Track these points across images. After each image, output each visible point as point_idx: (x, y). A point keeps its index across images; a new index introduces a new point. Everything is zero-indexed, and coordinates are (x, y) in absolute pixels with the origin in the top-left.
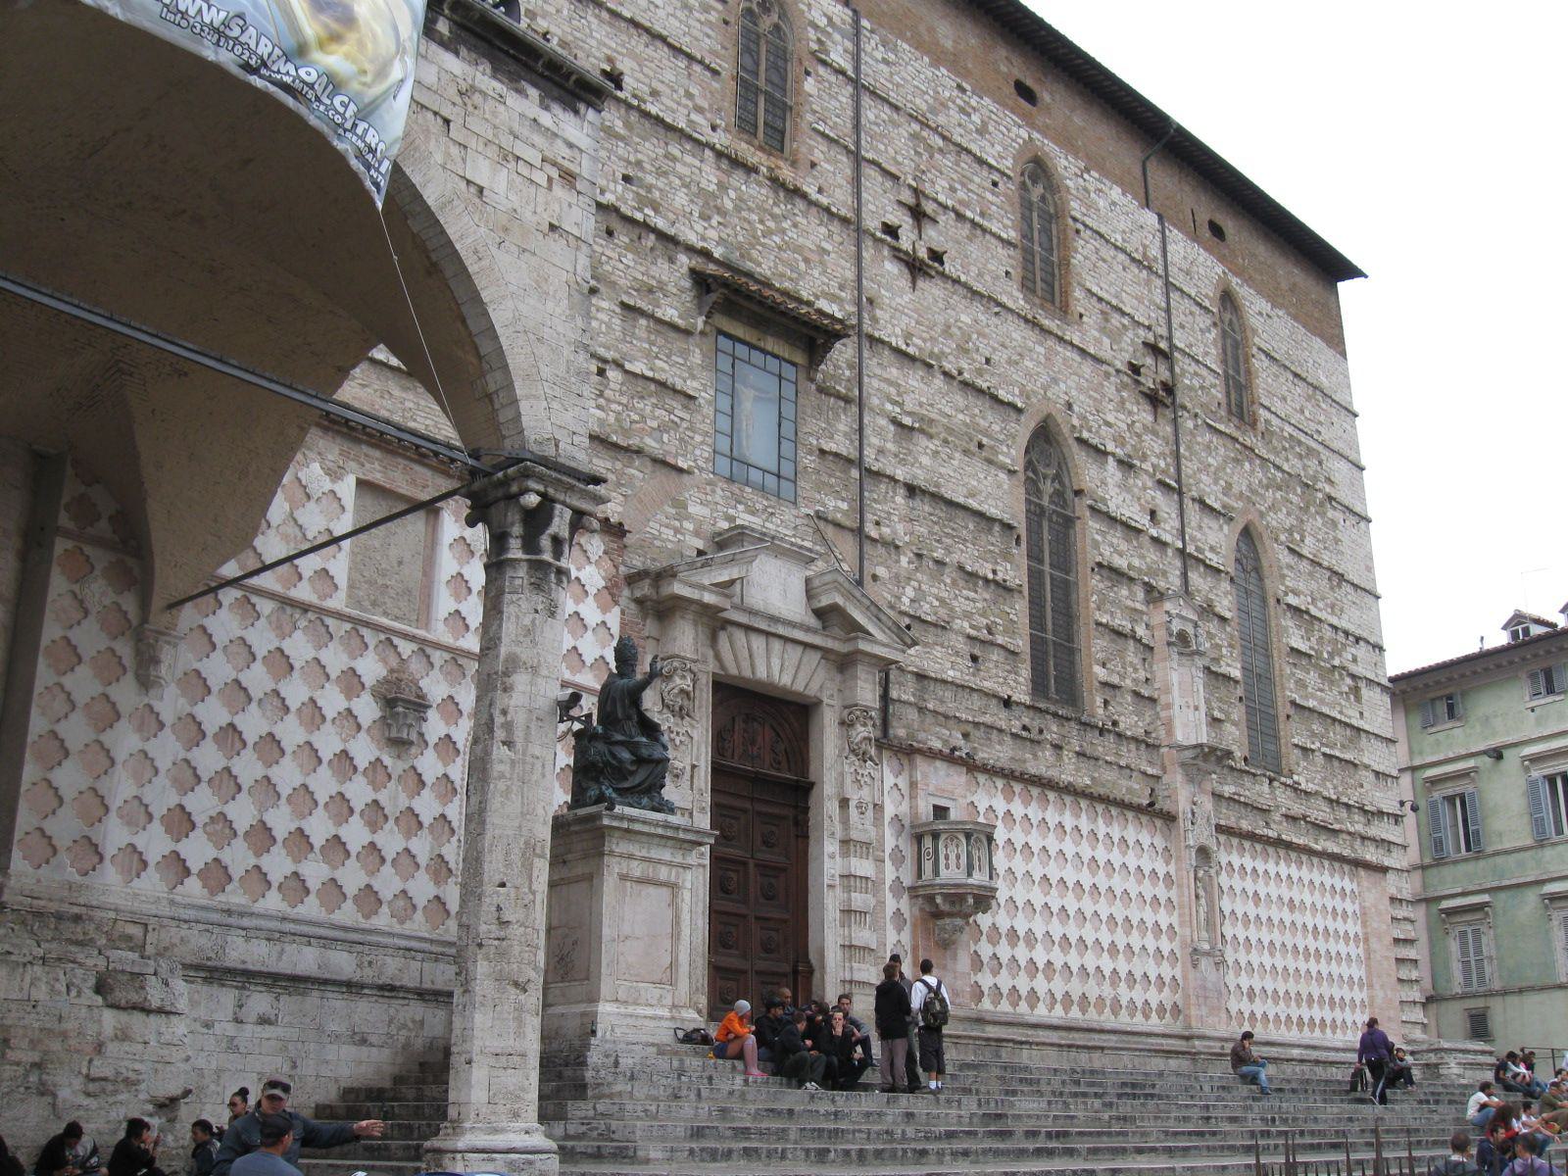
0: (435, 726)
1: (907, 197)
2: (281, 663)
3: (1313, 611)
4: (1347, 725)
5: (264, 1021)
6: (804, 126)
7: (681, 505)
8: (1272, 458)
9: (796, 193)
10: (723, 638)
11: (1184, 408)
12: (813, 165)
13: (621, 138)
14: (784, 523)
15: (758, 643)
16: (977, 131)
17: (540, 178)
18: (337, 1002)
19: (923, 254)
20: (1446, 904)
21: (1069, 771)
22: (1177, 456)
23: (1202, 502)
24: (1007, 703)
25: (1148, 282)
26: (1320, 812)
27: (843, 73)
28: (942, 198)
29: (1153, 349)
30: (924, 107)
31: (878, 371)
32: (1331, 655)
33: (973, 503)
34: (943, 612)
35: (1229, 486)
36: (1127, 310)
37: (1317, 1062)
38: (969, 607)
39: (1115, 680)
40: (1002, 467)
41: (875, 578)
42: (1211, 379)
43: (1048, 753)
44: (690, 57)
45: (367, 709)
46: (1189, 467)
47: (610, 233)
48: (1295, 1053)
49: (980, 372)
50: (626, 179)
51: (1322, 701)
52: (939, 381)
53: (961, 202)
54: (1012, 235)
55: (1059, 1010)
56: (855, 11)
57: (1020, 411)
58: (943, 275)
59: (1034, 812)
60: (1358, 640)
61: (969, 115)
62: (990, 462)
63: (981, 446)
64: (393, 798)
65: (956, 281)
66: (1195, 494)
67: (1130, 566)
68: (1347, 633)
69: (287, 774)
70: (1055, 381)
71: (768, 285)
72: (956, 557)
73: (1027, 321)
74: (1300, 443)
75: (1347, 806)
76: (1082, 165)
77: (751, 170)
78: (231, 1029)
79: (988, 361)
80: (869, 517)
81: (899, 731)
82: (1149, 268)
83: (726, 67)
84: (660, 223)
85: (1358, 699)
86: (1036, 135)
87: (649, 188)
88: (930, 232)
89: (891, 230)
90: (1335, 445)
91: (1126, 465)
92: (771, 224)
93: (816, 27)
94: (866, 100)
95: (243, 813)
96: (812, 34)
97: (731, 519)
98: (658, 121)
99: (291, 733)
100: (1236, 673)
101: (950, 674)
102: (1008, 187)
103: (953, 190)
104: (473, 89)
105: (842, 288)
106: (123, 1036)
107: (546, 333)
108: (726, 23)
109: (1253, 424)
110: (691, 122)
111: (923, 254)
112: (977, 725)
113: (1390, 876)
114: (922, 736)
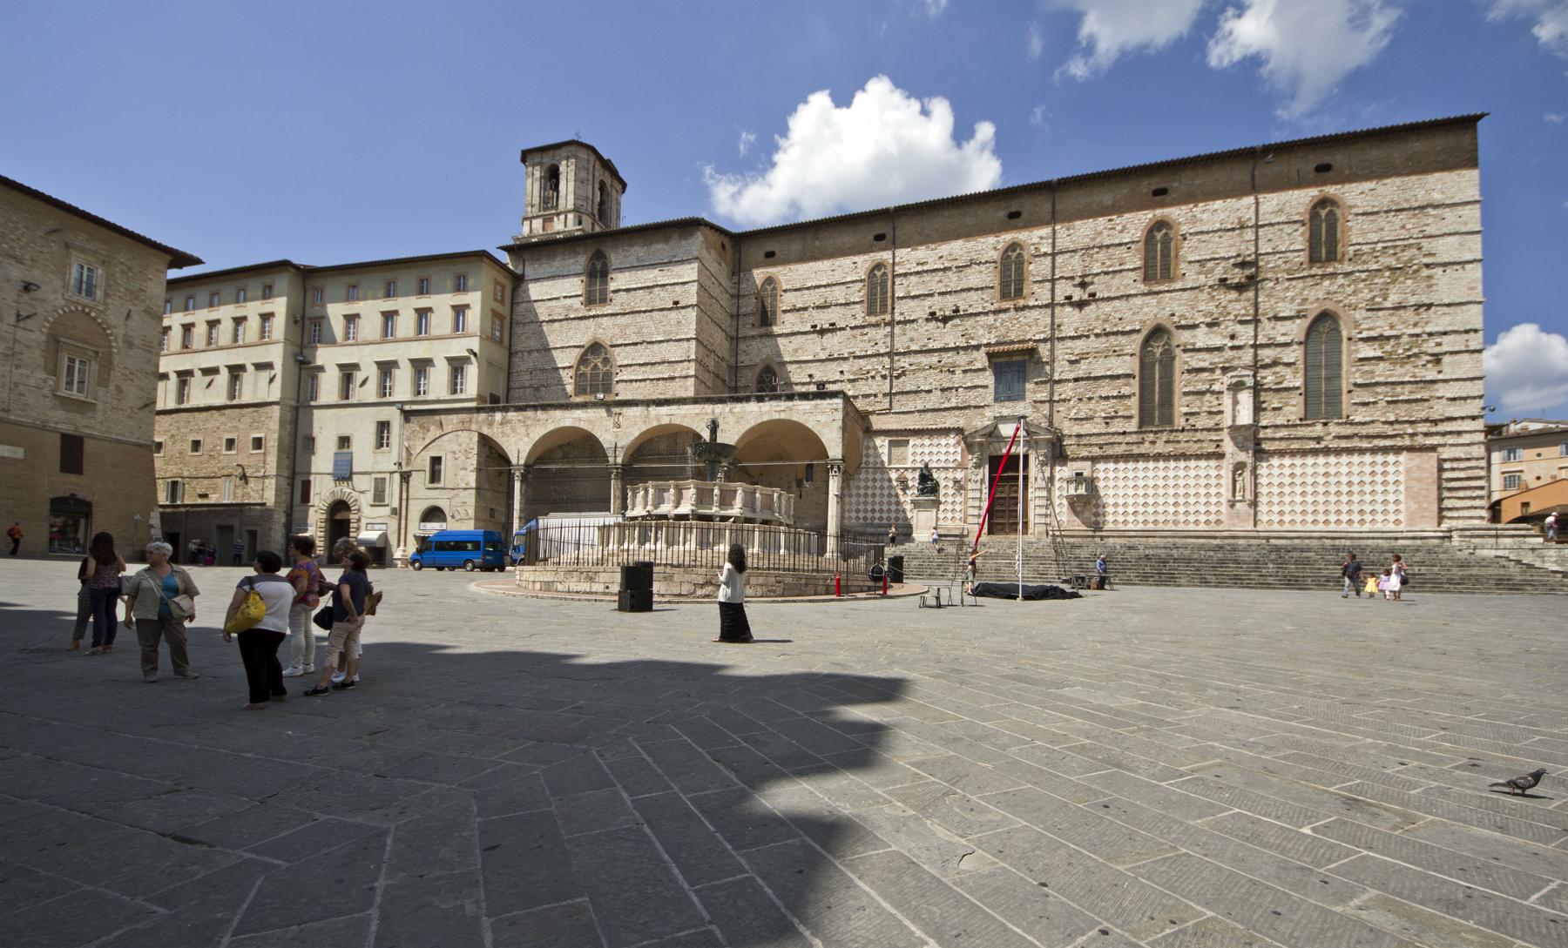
2: (874, 480)
7: (983, 415)
14: (1020, 408)
19: (1085, 297)
21: (1160, 448)
24: (1124, 433)
33: (1109, 373)
34: (1091, 413)
38: (1103, 408)
40: (1126, 355)
62: (1119, 356)
63: (1115, 351)
65: (1103, 299)
67: (1211, 364)
69: (878, 499)
71: (1012, 342)
72: (1098, 394)
80: (1056, 394)
83: (996, 283)
84: (973, 343)
91: (1209, 325)
93: (1034, 244)
95: (869, 507)
96: (1032, 248)
99: (878, 492)
100: (1297, 384)
110: (984, 308)
112: (1107, 444)
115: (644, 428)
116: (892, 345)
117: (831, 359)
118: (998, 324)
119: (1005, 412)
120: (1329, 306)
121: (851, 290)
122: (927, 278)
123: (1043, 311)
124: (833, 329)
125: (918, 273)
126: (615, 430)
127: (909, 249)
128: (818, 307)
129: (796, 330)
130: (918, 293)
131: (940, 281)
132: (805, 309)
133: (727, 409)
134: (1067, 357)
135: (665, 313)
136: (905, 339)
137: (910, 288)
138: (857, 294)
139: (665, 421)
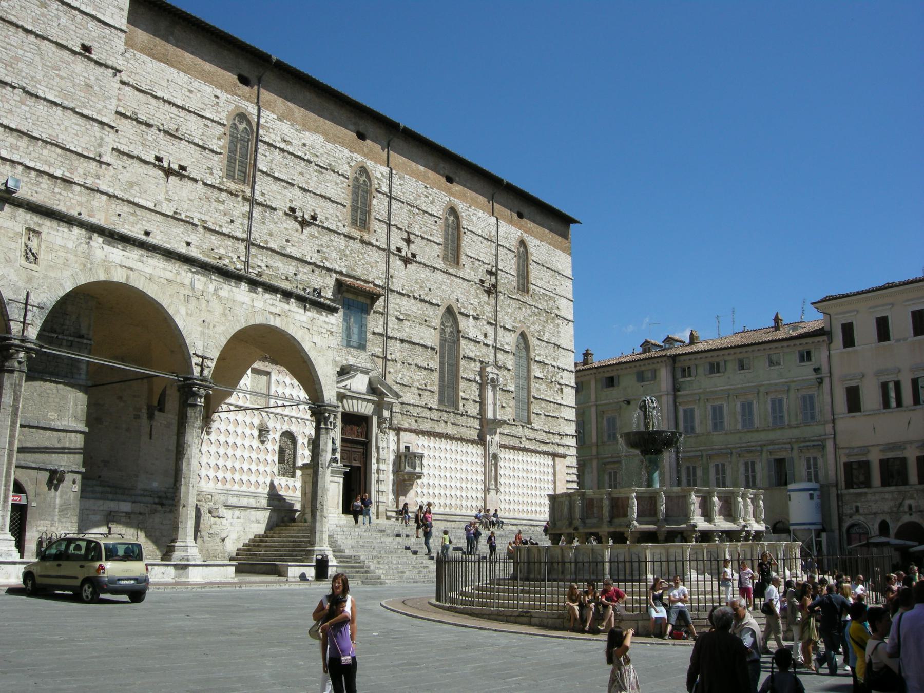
0: (270, 437)
1: (405, 235)
3: (546, 361)
4: (555, 403)
5: (238, 518)
6: (372, 218)
8: (534, 304)
9: (370, 244)
10: (345, 401)
11: (500, 292)
12: (375, 231)
13: (317, 237)
15: (355, 402)
16: (432, 203)
17: (326, 336)
18: (253, 512)
20: (605, 461)
21: (450, 430)
22: (496, 311)
23: (505, 328)
24: (430, 409)
25: (490, 246)
26: (541, 436)
27: (386, 194)
28: (417, 233)
29: (490, 273)
30: (412, 198)
31: (393, 301)
32: (552, 377)
33: (422, 342)
35: (516, 318)
36: (481, 259)
37: (531, 525)
38: (420, 377)
39: (467, 397)
41: (389, 372)
42: (512, 278)
43: (443, 424)
44: (337, 203)
45: (256, 433)
46: (500, 315)
47: (313, 271)
48: (524, 522)
49: (427, 294)
50: (318, 251)
51: (546, 395)
52: (413, 301)
53: (424, 232)
54: (440, 240)
55: (442, 509)
56: (390, 168)
57: (439, 306)
58: (416, 262)
59: (437, 445)
60: (563, 370)
61: (428, 197)
63: (426, 321)
64: (262, 456)
65: (420, 263)
66: (502, 325)
68: (559, 368)
70: (453, 292)
71: (359, 279)
72: (415, 362)
73: (444, 272)
74: (547, 295)
75: (553, 433)
76: (468, 205)
77: (354, 239)
78: (231, 520)
79: (430, 290)
80: (388, 352)
81: (395, 422)
82: (491, 241)
83: (348, 203)
84: (328, 265)
85: (562, 392)
86: (452, 198)
87: (324, 253)
88: (412, 246)
89: (399, 250)
90: (561, 294)
92: (361, 256)
93: (377, 178)
94: (393, 201)
97: (347, 360)
98: (328, 229)
100: (512, 389)
101: (412, 402)
102: (440, 222)
103: (421, 228)
104: (313, 319)
105: (382, 274)
106: (215, 524)
107: (328, 374)
108: (349, 186)
109: (528, 292)
111: (409, 255)
112: (419, 417)
113: (568, 458)
114: (402, 422)
115: (83, 280)
116: (249, 232)
117: (175, 217)
118: (348, 253)
119: (352, 361)
120: (524, 329)
121: (210, 132)
122: (290, 161)
123: (381, 252)
124: (181, 173)
125: (282, 150)
126: (23, 262)
127: (276, 117)
128: (167, 133)
129: (135, 153)
130: (282, 177)
131: (301, 174)
132: (149, 125)
133: (211, 288)
134: (396, 313)
135: (66, 54)
136: (264, 229)
137: (274, 166)
138: (215, 141)
139: (119, 276)
